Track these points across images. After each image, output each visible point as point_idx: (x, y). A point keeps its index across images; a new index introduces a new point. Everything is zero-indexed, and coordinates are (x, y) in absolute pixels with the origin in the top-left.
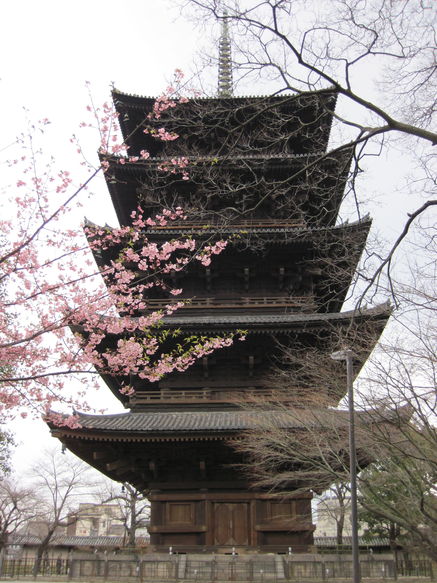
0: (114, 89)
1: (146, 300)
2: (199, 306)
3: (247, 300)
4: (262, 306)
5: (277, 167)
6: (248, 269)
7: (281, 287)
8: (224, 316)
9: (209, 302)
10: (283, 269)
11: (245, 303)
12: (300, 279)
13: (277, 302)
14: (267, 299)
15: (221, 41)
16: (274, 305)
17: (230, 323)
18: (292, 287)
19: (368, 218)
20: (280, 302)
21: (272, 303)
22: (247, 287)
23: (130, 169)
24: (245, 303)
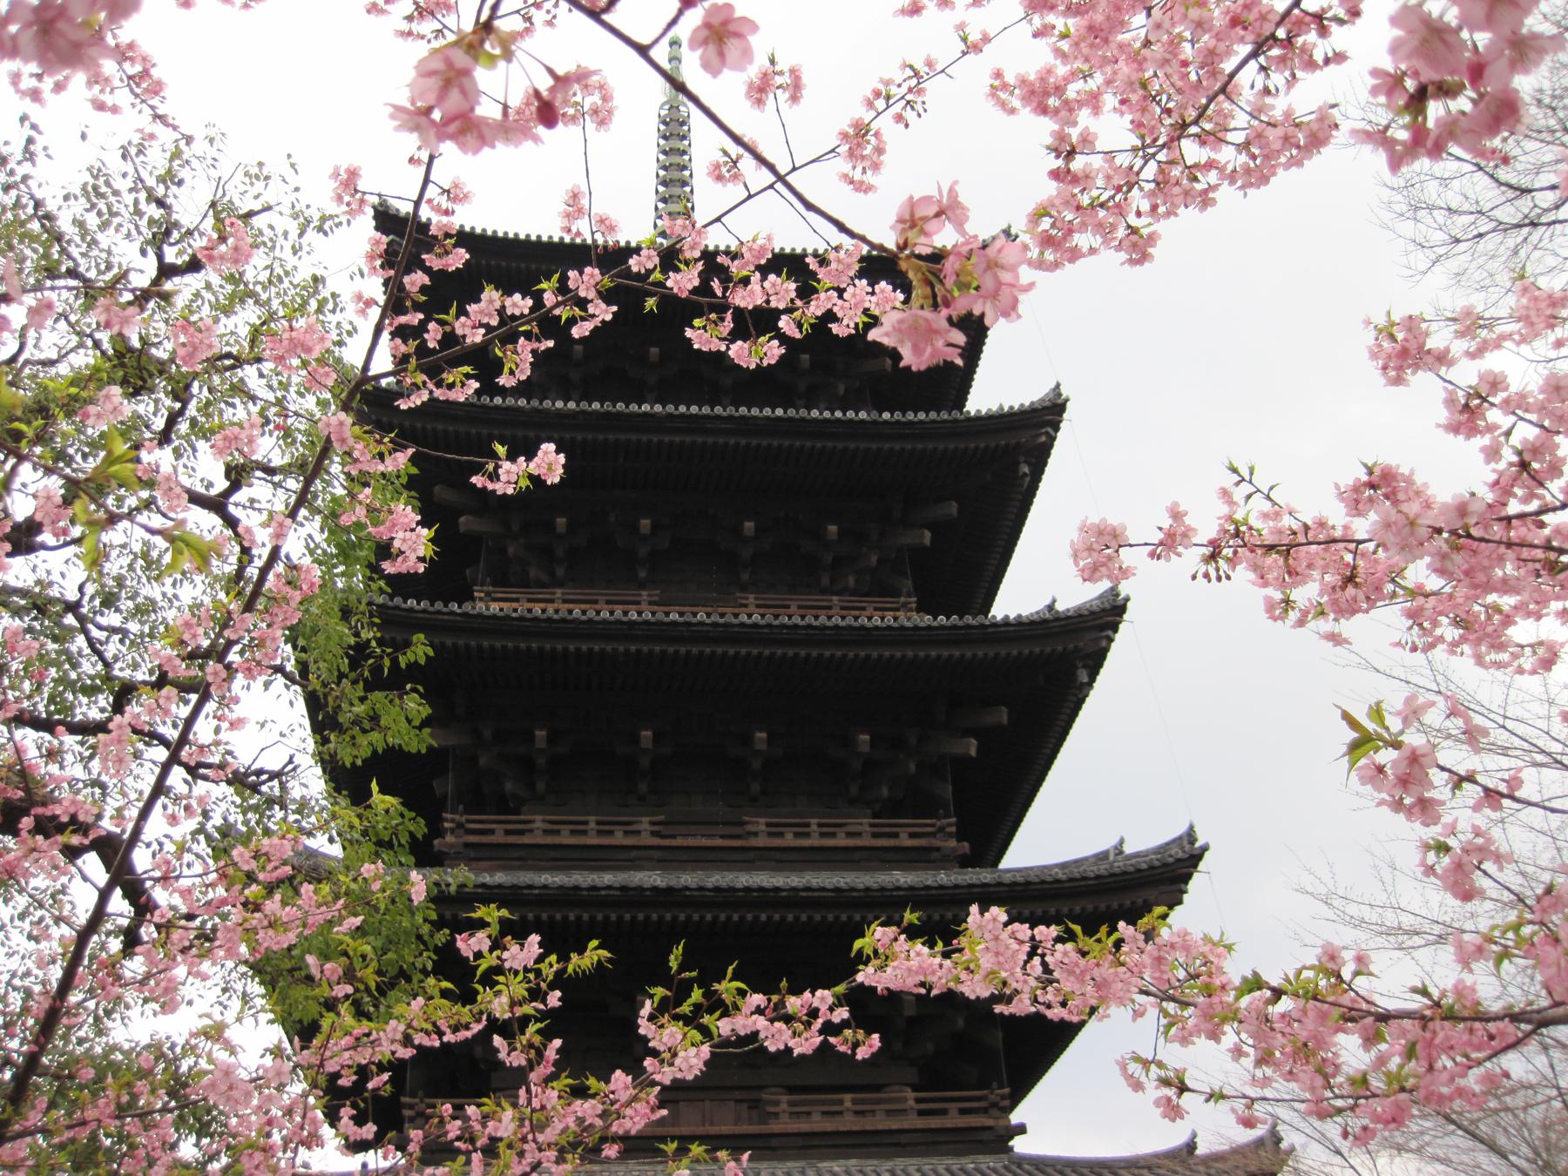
0: (383, 203)
1: (457, 817)
2: (619, 839)
3: (760, 824)
4: (806, 843)
5: (852, 446)
6: (764, 735)
7: (854, 790)
8: (694, 870)
9: (645, 831)
10: (867, 737)
11: (756, 834)
12: (912, 767)
13: (849, 835)
14: (820, 825)
15: (663, 113)
16: (841, 841)
17: (732, 890)
18: (885, 792)
19: (1118, 595)
20: (858, 834)
21: (833, 835)
22: (756, 788)
23: (424, 428)
24: (756, 834)
